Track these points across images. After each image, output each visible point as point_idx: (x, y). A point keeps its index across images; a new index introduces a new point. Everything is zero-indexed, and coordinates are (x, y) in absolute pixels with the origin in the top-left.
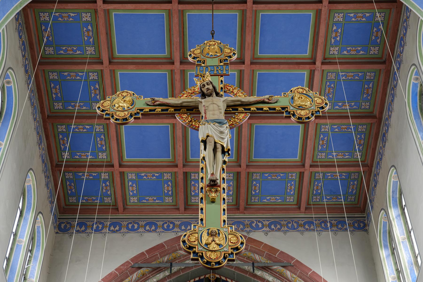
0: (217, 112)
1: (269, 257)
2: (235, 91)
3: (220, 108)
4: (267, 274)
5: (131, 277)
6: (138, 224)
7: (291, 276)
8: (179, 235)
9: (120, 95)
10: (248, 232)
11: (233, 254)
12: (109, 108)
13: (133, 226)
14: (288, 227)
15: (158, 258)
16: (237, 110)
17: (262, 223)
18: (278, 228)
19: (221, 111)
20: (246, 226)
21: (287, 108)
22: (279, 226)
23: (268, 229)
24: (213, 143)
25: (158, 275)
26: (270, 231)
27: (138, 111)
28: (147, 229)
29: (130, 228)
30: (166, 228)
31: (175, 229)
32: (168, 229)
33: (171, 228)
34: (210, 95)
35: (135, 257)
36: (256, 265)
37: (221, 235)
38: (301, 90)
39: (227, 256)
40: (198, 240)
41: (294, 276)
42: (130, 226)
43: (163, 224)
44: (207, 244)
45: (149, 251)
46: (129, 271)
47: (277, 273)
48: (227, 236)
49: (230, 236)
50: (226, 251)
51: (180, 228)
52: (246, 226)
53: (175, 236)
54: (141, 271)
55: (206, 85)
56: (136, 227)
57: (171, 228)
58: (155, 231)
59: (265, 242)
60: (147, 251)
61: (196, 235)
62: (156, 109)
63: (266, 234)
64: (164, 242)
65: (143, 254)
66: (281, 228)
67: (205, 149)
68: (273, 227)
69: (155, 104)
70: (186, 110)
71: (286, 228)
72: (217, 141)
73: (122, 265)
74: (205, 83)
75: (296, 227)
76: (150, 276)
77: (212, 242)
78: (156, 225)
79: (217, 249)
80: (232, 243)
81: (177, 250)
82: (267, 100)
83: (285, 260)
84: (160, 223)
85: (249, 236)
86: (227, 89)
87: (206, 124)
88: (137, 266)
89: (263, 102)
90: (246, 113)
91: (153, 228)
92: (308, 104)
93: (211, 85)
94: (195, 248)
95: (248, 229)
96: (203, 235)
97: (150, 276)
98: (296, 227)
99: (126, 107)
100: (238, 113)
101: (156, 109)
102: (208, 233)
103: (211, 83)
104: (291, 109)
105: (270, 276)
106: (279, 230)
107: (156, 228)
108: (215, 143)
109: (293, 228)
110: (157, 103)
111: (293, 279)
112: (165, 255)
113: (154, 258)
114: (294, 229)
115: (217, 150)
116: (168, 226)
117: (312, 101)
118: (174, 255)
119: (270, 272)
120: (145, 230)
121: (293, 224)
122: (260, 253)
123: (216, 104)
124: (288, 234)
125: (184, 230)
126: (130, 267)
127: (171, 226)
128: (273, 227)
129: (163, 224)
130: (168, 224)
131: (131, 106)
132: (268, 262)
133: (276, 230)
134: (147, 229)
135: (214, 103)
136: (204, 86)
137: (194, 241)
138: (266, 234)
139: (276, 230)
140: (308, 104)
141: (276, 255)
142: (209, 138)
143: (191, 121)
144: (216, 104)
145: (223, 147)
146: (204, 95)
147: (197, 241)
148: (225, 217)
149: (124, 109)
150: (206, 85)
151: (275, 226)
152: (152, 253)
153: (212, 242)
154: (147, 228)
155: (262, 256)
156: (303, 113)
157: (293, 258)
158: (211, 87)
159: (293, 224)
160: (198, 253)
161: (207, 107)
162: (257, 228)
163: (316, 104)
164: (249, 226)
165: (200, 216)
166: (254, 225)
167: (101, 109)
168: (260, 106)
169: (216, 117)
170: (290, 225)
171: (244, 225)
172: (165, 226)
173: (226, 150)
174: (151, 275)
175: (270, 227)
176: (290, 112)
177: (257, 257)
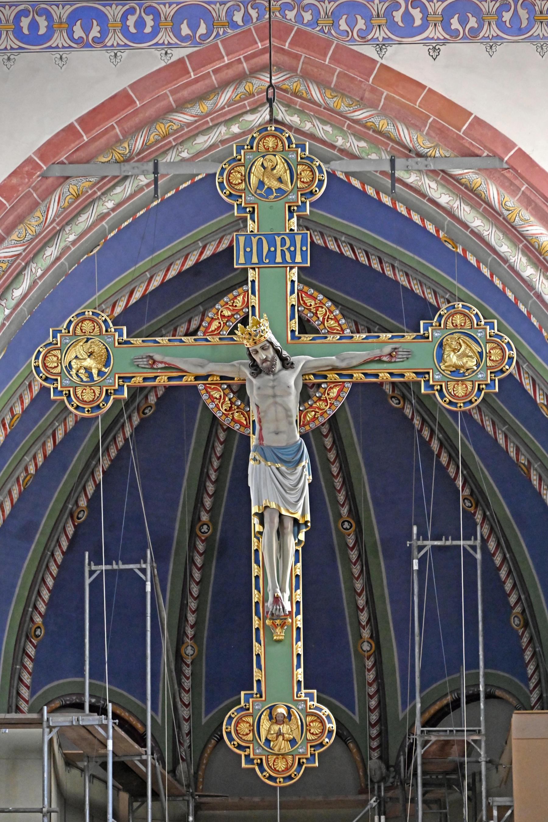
0: (283, 426)
1: (441, 134)
2: (321, 313)
3: (289, 413)
4: (433, 185)
5: (43, 208)
6: (49, 17)
7: (500, 203)
8: (174, 59)
9: (78, 331)
10: (381, 47)
11: (315, 754)
12: (59, 374)
13: (34, 25)
14: (501, 25)
15: (119, 141)
16: (325, 377)
17: (424, 10)
18: (471, 28)
19: (290, 419)
20: (375, 22)
21: (428, 373)
22: (473, 22)
23: (440, 33)
24: (277, 520)
25: (118, 190)
26: (445, 42)
27: (121, 383)
28: (76, 36)
29: (26, 31)
30: (133, 30)
31: (163, 37)
32: (139, 37)
33: (148, 30)
34: (270, 371)
35: (49, 143)
36: (399, 162)
37: (293, 717)
38: (458, 319)
39: (303, 763)
40: (253, 730)
41: (511, 202)
42: (25, 22)
43: (124, 17)
44: (268, 741)
45: (89, 120)
46: (35, 189)
47: (462, 184)
48: (304, 721)
49: (309, 719)
50: (303, 754)
51: (177, 33)
52: (375, 22)
53: (163, 64)
54: (70, 188)
55: (259, 350)
56: (42, 31)
57: (148, 30)
58: (99, 41)
59: (429, 85)
60: (82, 120)
61: (250, 720)
62: (156, 377)
63: (435, 52)
64: (132, 86)
65: (71, 127)
66: (481, 27)
67: (262, 523)
68: (455, 24)
69: (155, 367)
70: (218, 378)
71: (495, 31)
72: (284, 512)
73: (14, 173)
74: (258, 347)
75: (524, 24)
76: (95, 192)
77: (277, 737)
78: (102, 19)
79: (287, 751)
80: (312, 734)
81: (171, 110)
82: (385, 359)
83: (485, 147)
84: (114, 12)
85: (384, 62)
86: (305, 303)
87: (263, 463)
88: (57, 171)
89: (379, 361)
90: (344, 382)
91: (95, 32)
92: (472, 363)
93: (271, 350)
94: (249, 747)
95: (379, 34)
96: (262, 720)
97: (95, 192)
98: (524, 24)
99: (95, 372)
100: (326, 383)
101: (156, 377)
102: (271, 713)
103: (271, 343)
104: (435, 377)
105: (440, 190)
106: (474, 34)
107: (104, 33)
108: (281, 515)
109: (517, 30)
110: (160, 366)
111: (506, 213)
112: (138, 129)
113: (103, 140)
114: (520, 31)
115: (285, 531)
116: (140, 24)
117: (481, 354)
118: (161, 128)
119: (443, 178)
120: (71, 38)
121: (516, 10)
122: (414, 120)
123: (281, 405)
124: (500, 49)
125: (187, 38)
126: (38, 177)
127: (149, 20)
128: (455, 24)
129: (124, 17)
130: (140, 16)
131: (107, 365)
132: (437, 155)
133: (464, 37)
134: (76, 36)
135: (276, 403)
136: (257, 352)
137: (247, 734)
138: (435, 52)
139: (464, 37)
140: (472, 363)
141: (460, 131)
142: (268, 509)
143: (231, 408)
144: (281, 405)
145: (295, 521)
146: (256, 369)
147: (251, 734)
148: (300, 674)
149: (91, 375)
150: (259, 350)
151: (463, 22)
152: (97, 128)
153: (277, 737)
154: (78, 32)
155: (419, 129)
156: (460, 391)
157: (508, 144)
158: (271, 353)
159: (516, 10)
160: (253, 759)
161: (265, 412)
162: (407, 31)
163: (489, 363)
164: (383, 21)
165: (257, 675)
166: (398, 16)
167: (44, 377)
168: (372, 368)
169: (281, 441)
170: (507, 16)
171: (368, 18)
172: (131, 21)
173: (301, 522)
174: (99, 189)
175: (447, 27)
176: (433, 386)
177: (405, 134)
